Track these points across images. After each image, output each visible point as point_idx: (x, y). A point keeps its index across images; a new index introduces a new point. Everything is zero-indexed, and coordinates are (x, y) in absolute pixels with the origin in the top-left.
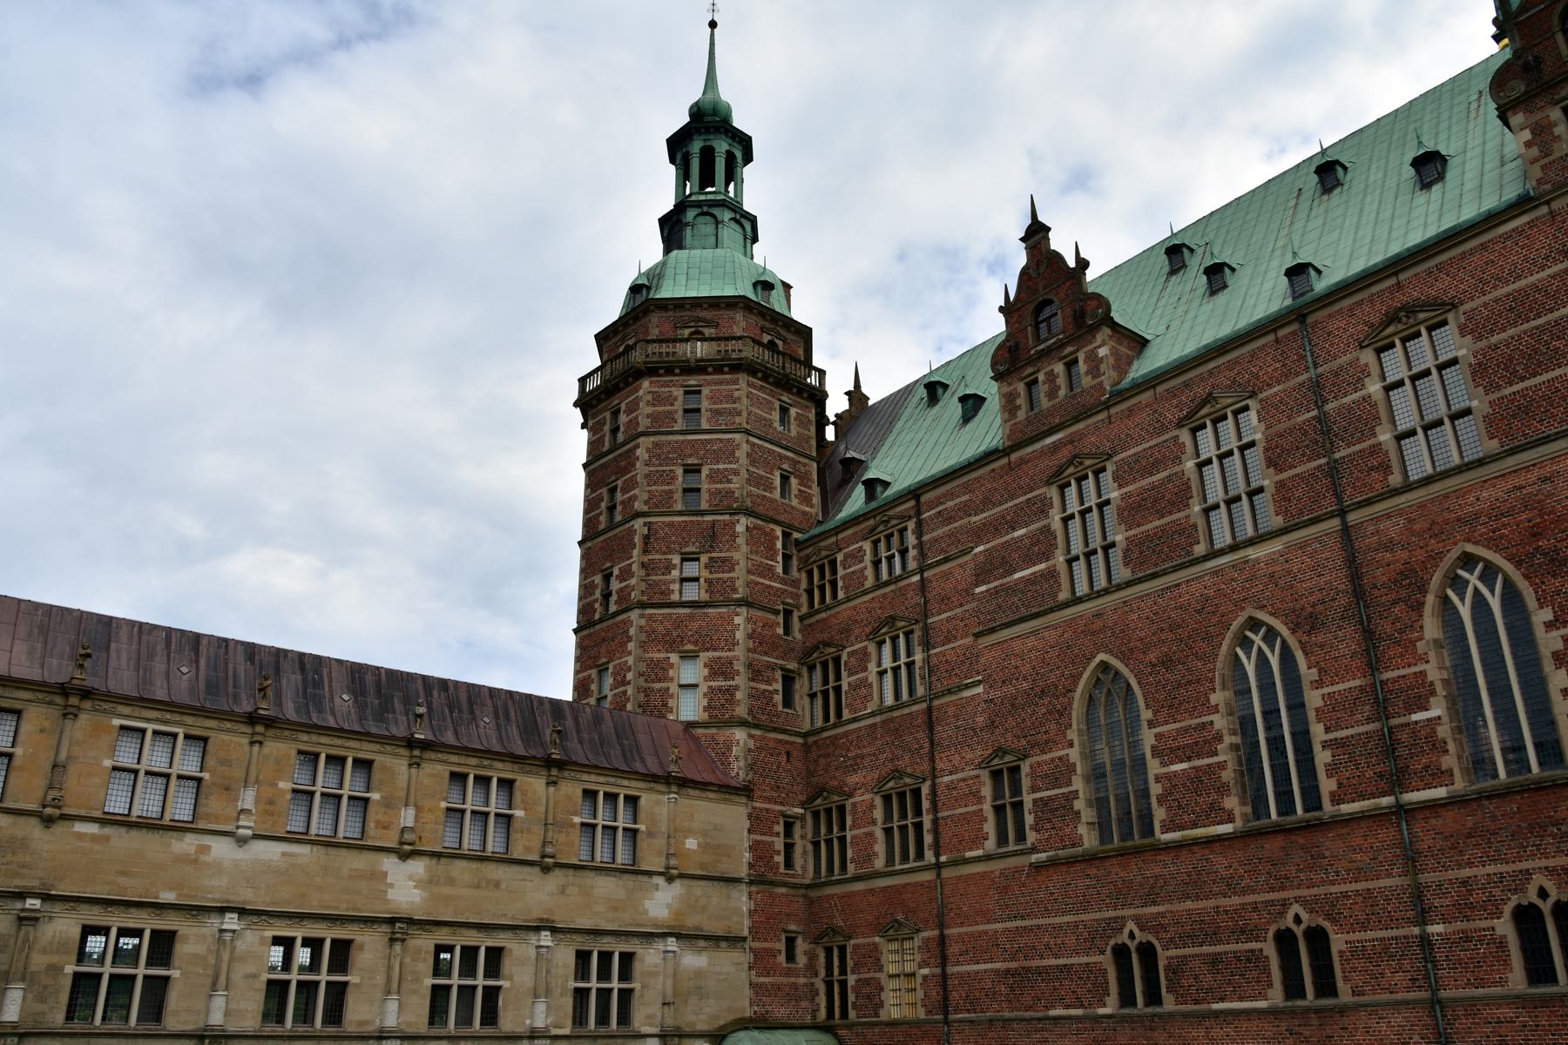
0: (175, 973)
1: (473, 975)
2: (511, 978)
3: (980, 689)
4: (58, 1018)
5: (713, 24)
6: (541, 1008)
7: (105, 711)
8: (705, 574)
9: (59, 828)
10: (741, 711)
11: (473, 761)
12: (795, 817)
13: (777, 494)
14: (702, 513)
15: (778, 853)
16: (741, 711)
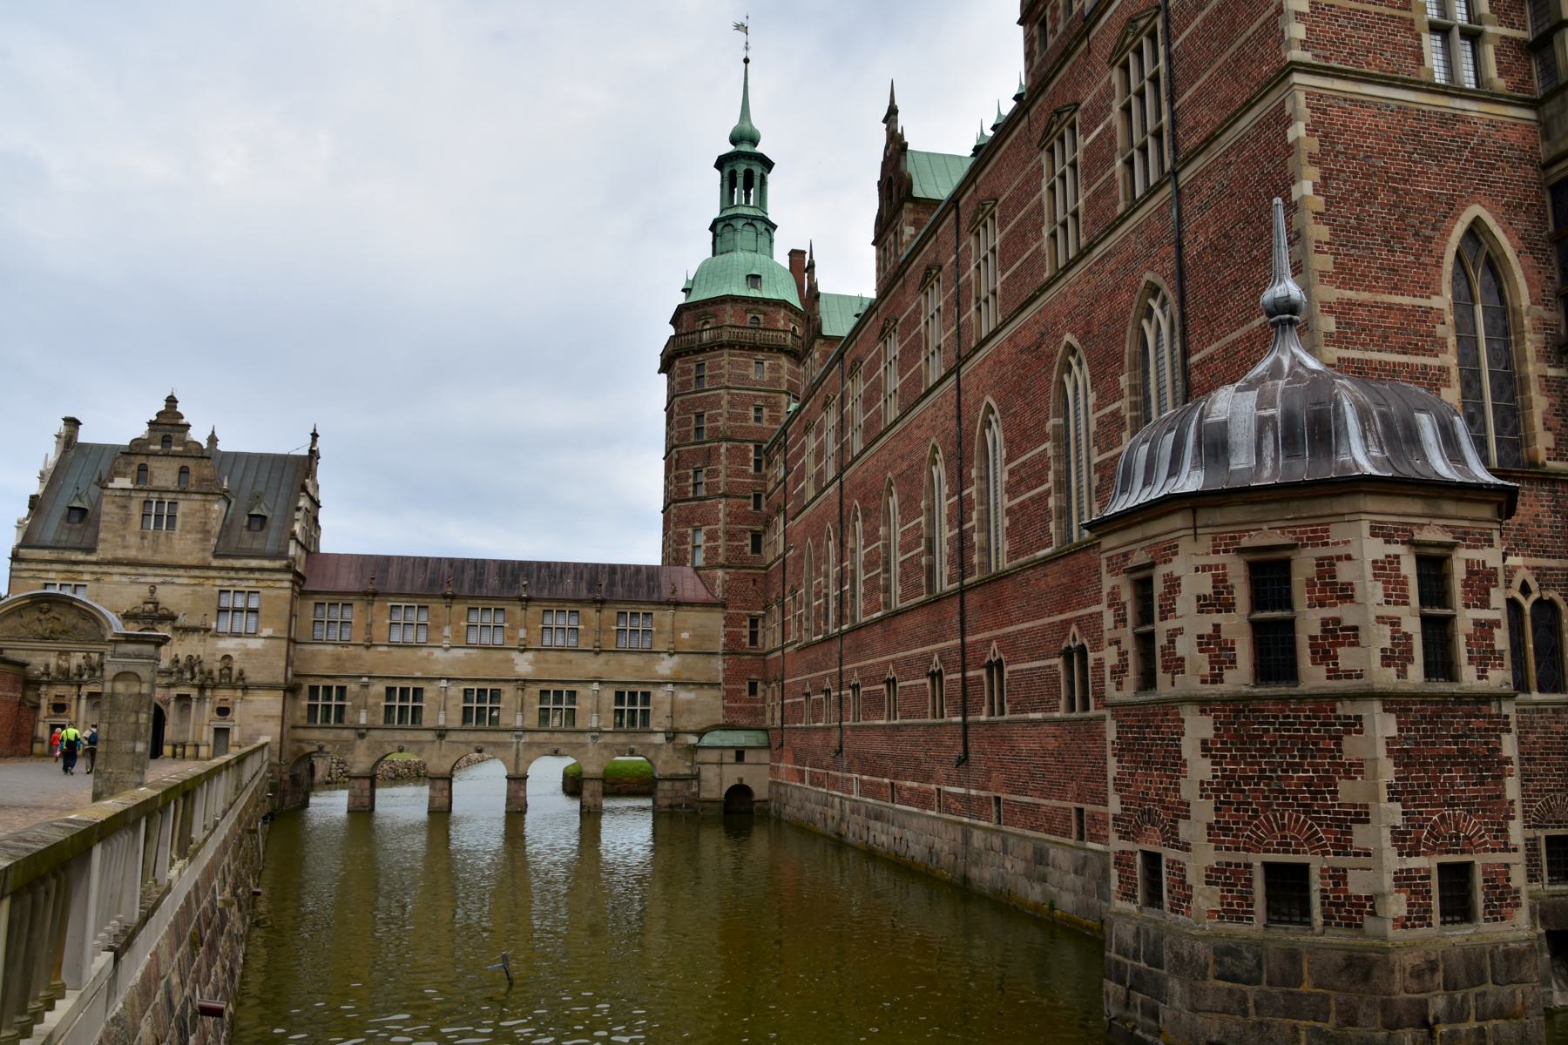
1: (623, 704)
4: (381, 722)
5: (746, 61)
6: (595, 718)
8: (705, 480)
9: (372, 649)
10: (721, 559)
12: (759, 616)
13: (752, 423)
16: (721, 559)
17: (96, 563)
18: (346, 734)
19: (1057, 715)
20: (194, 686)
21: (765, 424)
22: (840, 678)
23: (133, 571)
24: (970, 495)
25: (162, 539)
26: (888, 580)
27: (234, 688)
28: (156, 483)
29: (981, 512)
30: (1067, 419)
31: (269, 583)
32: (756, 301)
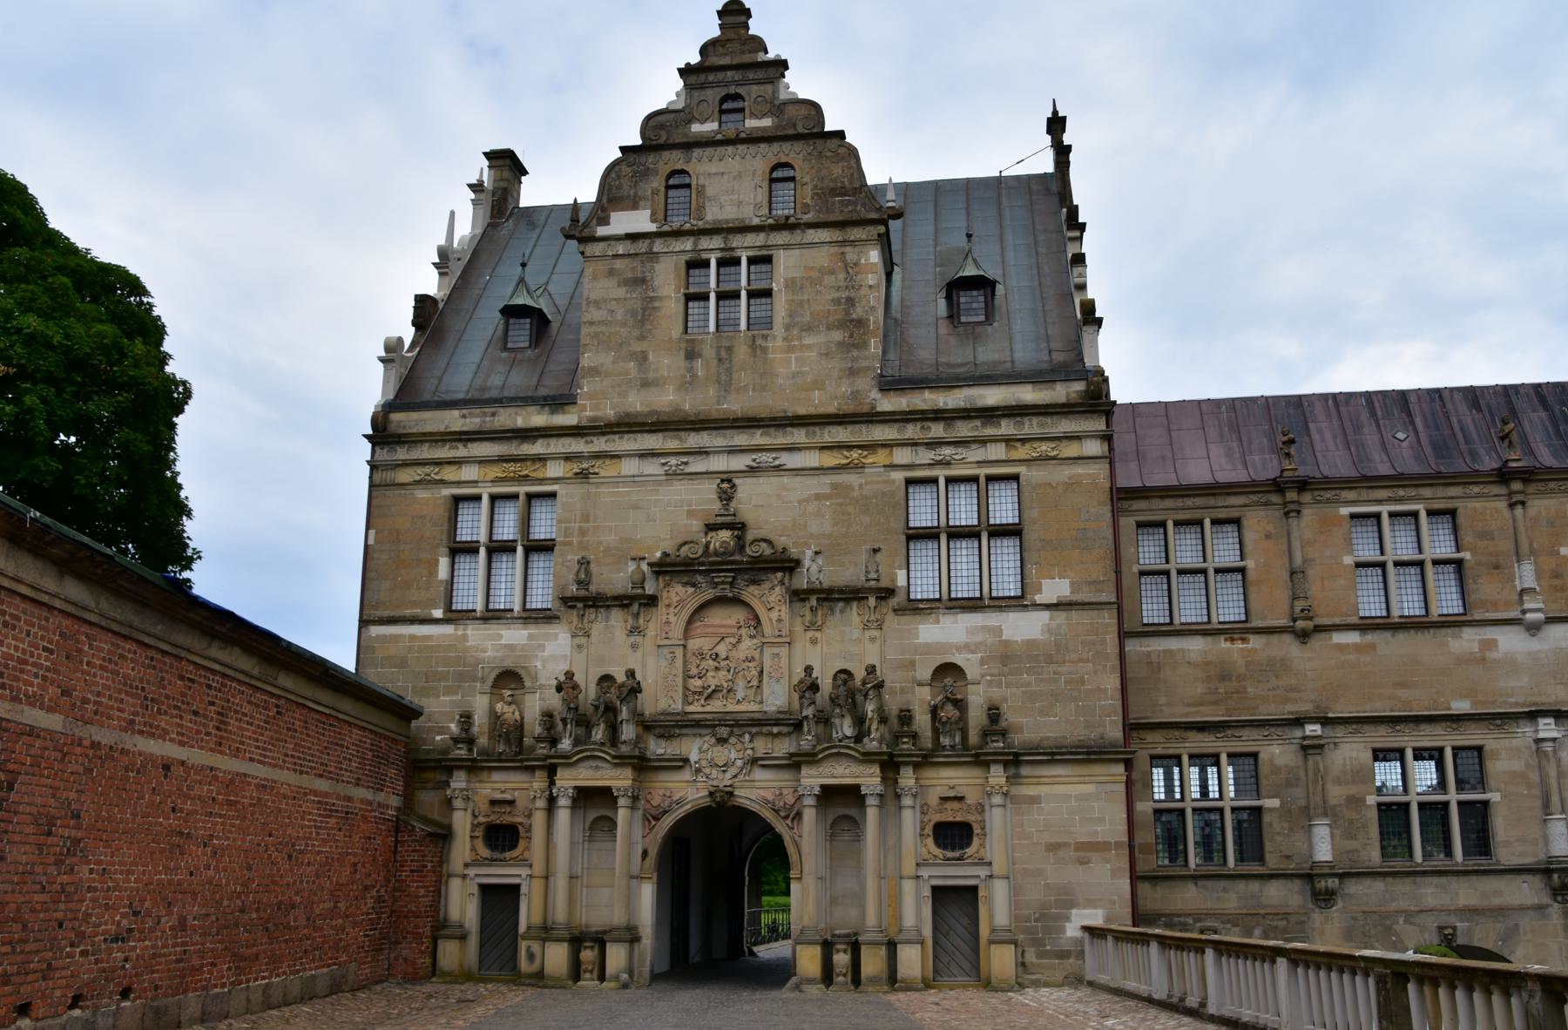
0: (1494, 797)
4: (1373, 855)
7: (1328, 501)
9: (1317, 642)
17: (576, 432)
18: (1277, 894)
20: (868, 758)
23: (672, 443)
25: (742, 351)
27: (981, 761)
28: (713, 214)
31: (1045, 447)
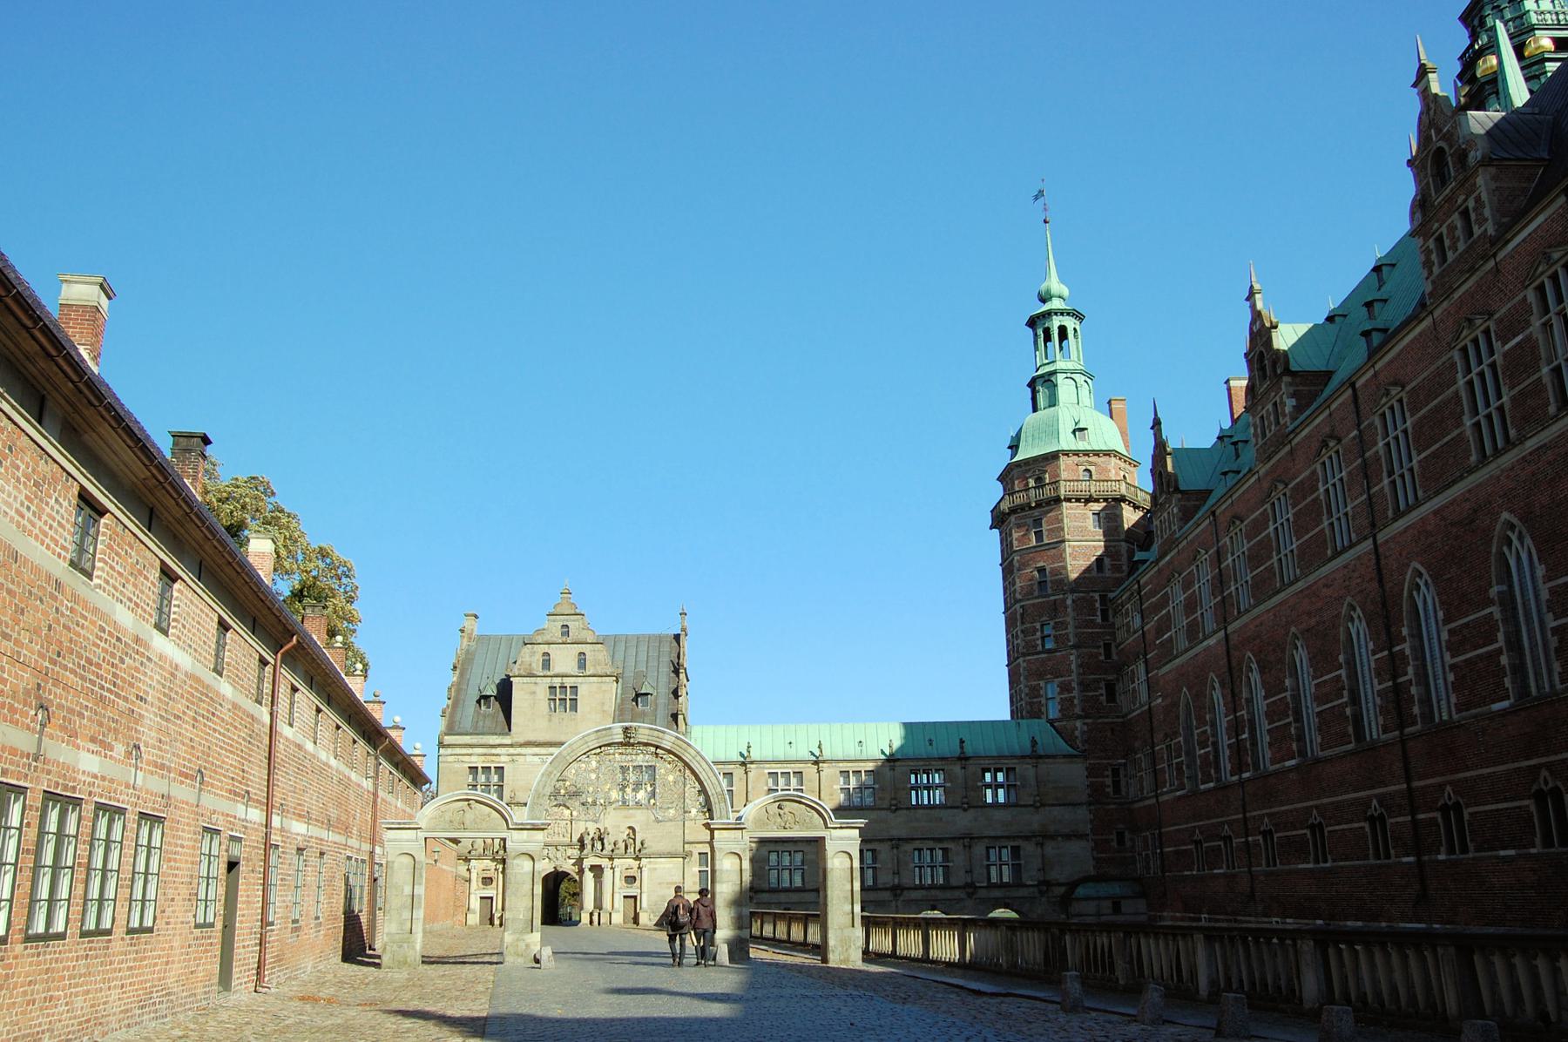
2: (953, 861)
3: (1160, 700)
8: (1053, 633)
11: (922, 763)
12: (1120, 764)
14: (1049, 596)
15: (1109, 786)
16: (1078, 710)
17: (511, 746)
19: (1533, 851)
21: (1108, 573)
22: (1246, 824)
24: (1402, 651)
26: (1301, 731)
29: (1416, 668)
30: (1511, 586)
32: (1086, 453)
